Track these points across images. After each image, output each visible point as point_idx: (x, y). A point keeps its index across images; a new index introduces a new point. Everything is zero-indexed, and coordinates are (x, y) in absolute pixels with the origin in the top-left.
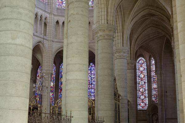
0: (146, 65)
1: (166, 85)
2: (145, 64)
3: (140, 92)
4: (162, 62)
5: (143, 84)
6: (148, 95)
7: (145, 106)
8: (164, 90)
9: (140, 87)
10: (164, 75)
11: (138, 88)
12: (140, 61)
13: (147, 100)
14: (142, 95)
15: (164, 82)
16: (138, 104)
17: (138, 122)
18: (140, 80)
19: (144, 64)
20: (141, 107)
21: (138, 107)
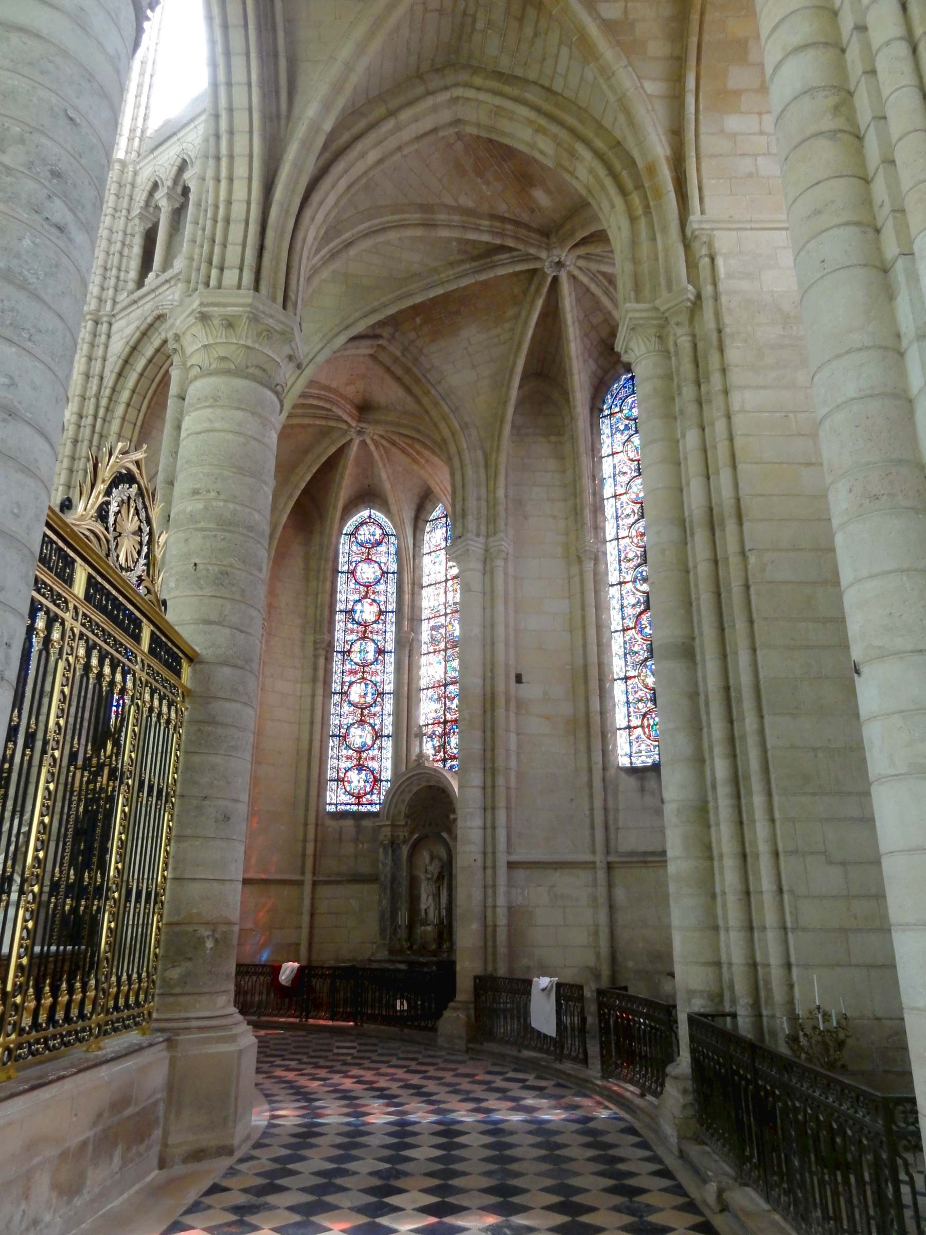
0: (398, 553)
1: (517, 631)
2: (393, 550)
3: (350, 703)
5: (370, 657)
6: (396, 724)
7: (371, 793)
8: (507, 666)
9: (352, 672)
11: (336, 678)
12: (364, 530)
13: (388, 753)
14: (362, 722)
17: (324, 892)
18: (353, 637)
19: (382, 548)
20: (345, 798)
21: (330, 797)
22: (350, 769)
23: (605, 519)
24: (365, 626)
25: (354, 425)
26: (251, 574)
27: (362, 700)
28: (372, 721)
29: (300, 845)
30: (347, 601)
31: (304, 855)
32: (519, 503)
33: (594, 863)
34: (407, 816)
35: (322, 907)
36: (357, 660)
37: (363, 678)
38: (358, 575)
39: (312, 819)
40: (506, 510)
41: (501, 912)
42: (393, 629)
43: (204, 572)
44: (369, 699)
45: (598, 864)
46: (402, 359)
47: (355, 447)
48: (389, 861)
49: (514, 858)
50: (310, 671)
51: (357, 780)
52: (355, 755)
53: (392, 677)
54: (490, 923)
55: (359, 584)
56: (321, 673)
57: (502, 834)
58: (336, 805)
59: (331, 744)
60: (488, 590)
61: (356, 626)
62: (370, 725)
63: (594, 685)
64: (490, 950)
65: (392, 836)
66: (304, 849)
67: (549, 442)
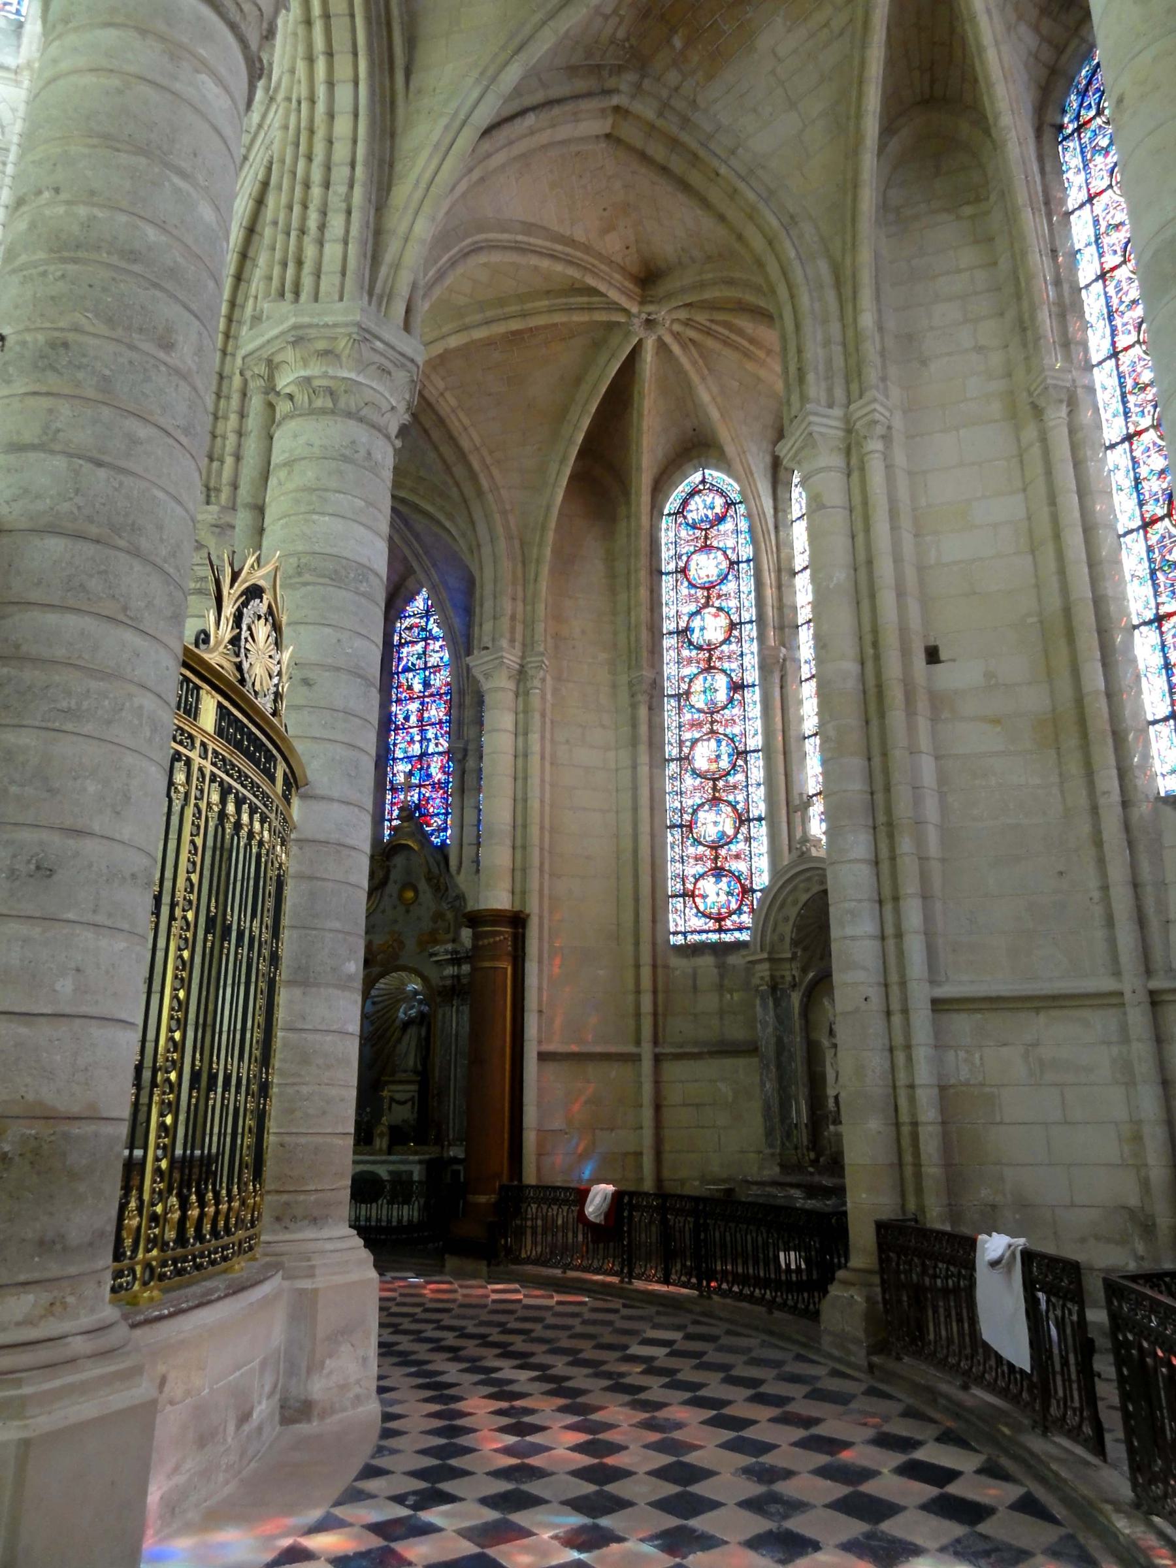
0: (751, 530)
1: (921, 569)
2: (744, 525)
3: (696, 773)
4: (866, 297)
5: (722, 697)
6: (770, 799)
7: (739, 911)
8: (903, 631)
10: (900, 458)
11: (670, 736)
13: (761, 846)
14: (715, 801)
15: (895, 528)
16: (674, 886)
17: (674, 1071)
18: (692, 669)
19: (728, 526)
20: (697, 923)
21: (675, 922)
22: (702, 876)
23: (1086, 326)
24: (709, 651)
25: (634, 309)
26: (132, 347)
27: (714, 766)
28: (731, 798)
29: (631, 998)
30: (678, 615)
31: (638, 1015)
32: (909, 339)
33: (1121, 994)
34: (795, 943)
35: (673, 1095)
36: (701, 705)
37: (712, 732)
38: (692, 573)
39: (646, 958)
40: (883, 354)
41: (927, 1099)
42: (755, 647)
43: (18, 348)
44: (724, 764)
45: (1128, 996)
46: (659, 123)
47: (649, 356)
48: (770, 1018)
49: (946, 991)
50: (626, 730)
51: (715, 893)
52: (708, 853)
53: (758, 724)
54: (904, 1117)
55: (694, 586)
56: (643, 729)
57: (915, 947)
58: (684, 934)
59: (670, 839)
60: (857, 500)
61: (694, 652)
62: (729, 803)
63: (1088, 641)
64: (909, 1171)
65: (772, 977)
66: (638, 1005)
67: (959, 218)
